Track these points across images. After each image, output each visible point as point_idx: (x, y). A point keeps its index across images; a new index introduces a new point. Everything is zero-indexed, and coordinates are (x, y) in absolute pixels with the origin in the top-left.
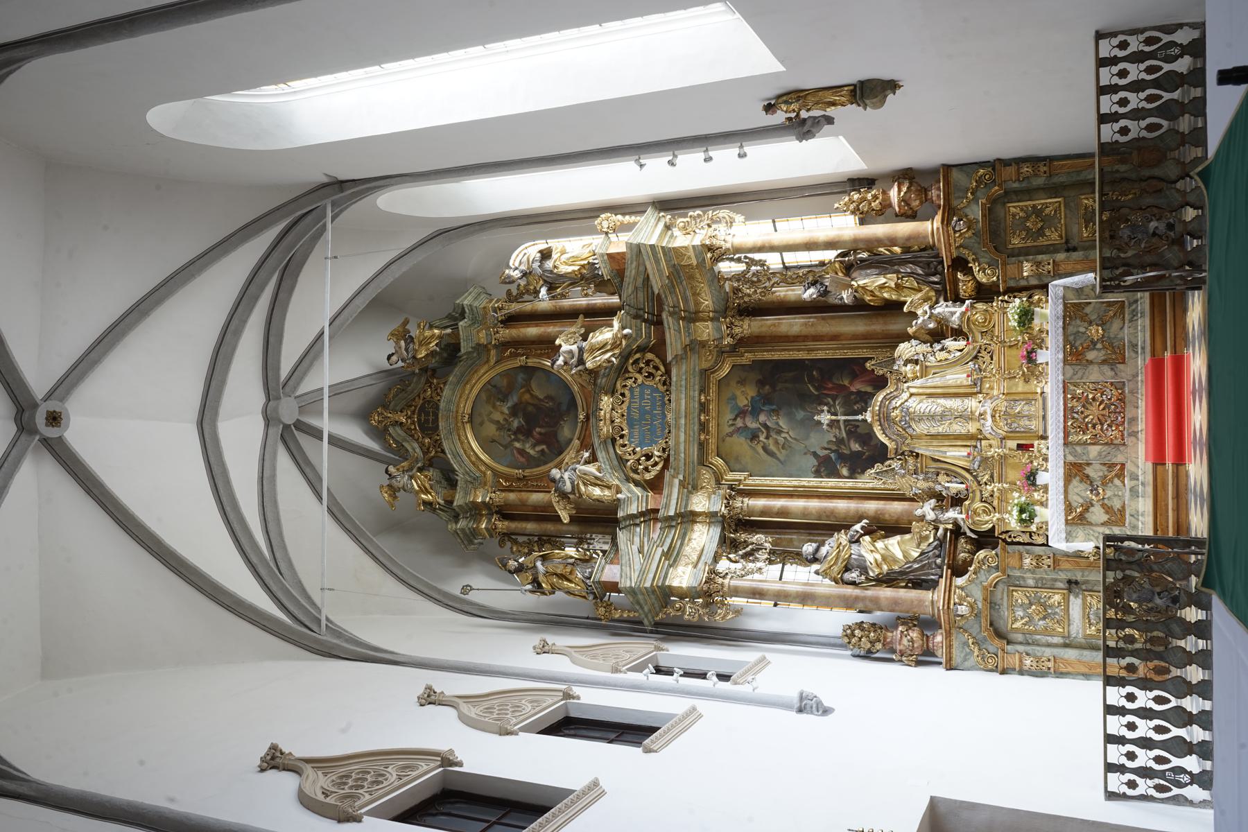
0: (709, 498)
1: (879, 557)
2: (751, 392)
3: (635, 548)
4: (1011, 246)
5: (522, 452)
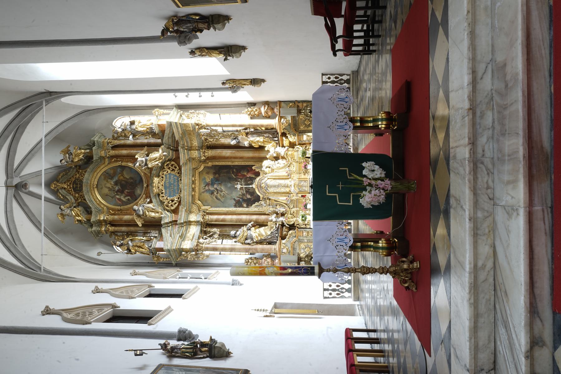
0: (196, 215)
1: (257, 235)
2: (211, 177)
3: (169, 235)
4: (300, 129)
5: (120, 199)
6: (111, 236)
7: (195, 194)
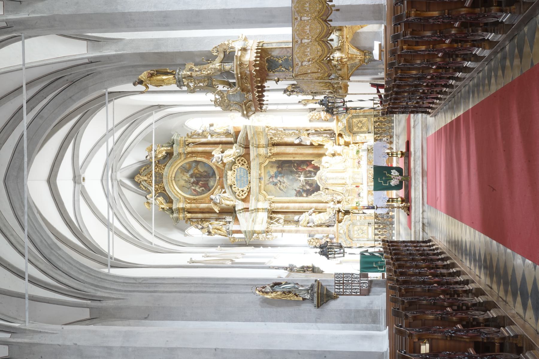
1: (318, 220)
5: (195, 190)
6: (186, 222)
7: (261, 185)
